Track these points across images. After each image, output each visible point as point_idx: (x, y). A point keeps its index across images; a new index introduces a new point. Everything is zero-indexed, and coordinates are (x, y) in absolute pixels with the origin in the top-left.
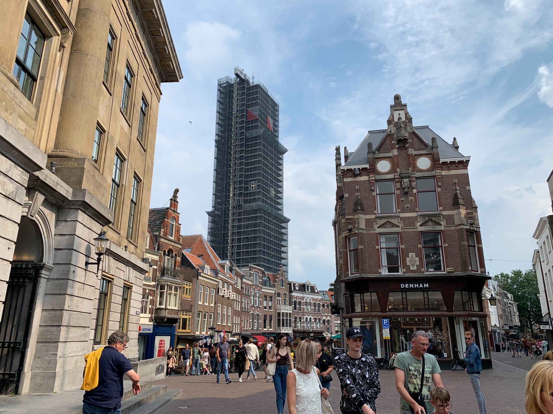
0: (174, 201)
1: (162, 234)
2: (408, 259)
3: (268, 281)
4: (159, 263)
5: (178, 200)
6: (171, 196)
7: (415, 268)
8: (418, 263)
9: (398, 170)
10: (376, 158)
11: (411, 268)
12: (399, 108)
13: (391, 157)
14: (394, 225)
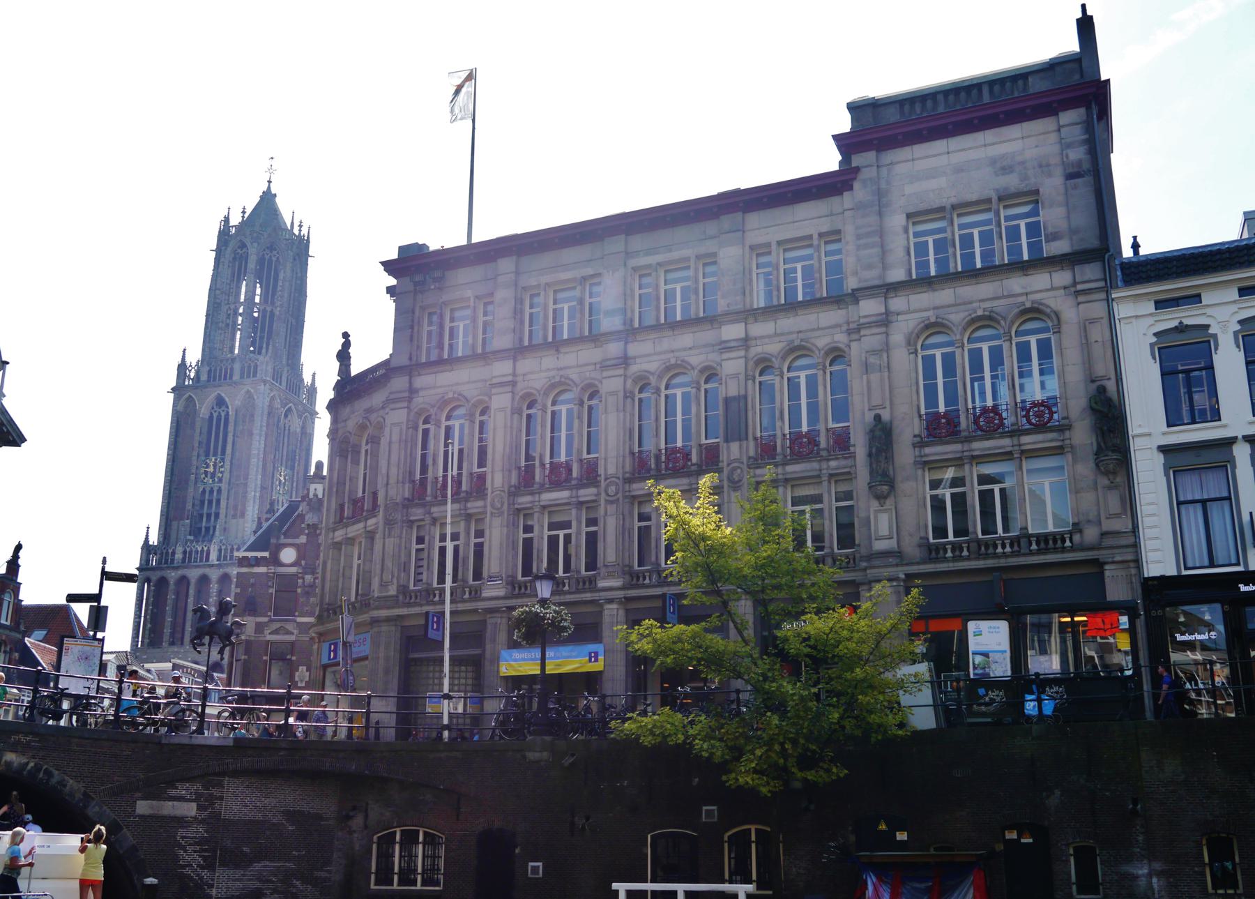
2: (297, 674)
5: (20, 562)
6: (9, 556)
7: (303, 685)
8: (307, 679)
9: (303, 562)
10: (280, 544)
11: (299, 685)
12: (317, 481)
13: (297, 544)
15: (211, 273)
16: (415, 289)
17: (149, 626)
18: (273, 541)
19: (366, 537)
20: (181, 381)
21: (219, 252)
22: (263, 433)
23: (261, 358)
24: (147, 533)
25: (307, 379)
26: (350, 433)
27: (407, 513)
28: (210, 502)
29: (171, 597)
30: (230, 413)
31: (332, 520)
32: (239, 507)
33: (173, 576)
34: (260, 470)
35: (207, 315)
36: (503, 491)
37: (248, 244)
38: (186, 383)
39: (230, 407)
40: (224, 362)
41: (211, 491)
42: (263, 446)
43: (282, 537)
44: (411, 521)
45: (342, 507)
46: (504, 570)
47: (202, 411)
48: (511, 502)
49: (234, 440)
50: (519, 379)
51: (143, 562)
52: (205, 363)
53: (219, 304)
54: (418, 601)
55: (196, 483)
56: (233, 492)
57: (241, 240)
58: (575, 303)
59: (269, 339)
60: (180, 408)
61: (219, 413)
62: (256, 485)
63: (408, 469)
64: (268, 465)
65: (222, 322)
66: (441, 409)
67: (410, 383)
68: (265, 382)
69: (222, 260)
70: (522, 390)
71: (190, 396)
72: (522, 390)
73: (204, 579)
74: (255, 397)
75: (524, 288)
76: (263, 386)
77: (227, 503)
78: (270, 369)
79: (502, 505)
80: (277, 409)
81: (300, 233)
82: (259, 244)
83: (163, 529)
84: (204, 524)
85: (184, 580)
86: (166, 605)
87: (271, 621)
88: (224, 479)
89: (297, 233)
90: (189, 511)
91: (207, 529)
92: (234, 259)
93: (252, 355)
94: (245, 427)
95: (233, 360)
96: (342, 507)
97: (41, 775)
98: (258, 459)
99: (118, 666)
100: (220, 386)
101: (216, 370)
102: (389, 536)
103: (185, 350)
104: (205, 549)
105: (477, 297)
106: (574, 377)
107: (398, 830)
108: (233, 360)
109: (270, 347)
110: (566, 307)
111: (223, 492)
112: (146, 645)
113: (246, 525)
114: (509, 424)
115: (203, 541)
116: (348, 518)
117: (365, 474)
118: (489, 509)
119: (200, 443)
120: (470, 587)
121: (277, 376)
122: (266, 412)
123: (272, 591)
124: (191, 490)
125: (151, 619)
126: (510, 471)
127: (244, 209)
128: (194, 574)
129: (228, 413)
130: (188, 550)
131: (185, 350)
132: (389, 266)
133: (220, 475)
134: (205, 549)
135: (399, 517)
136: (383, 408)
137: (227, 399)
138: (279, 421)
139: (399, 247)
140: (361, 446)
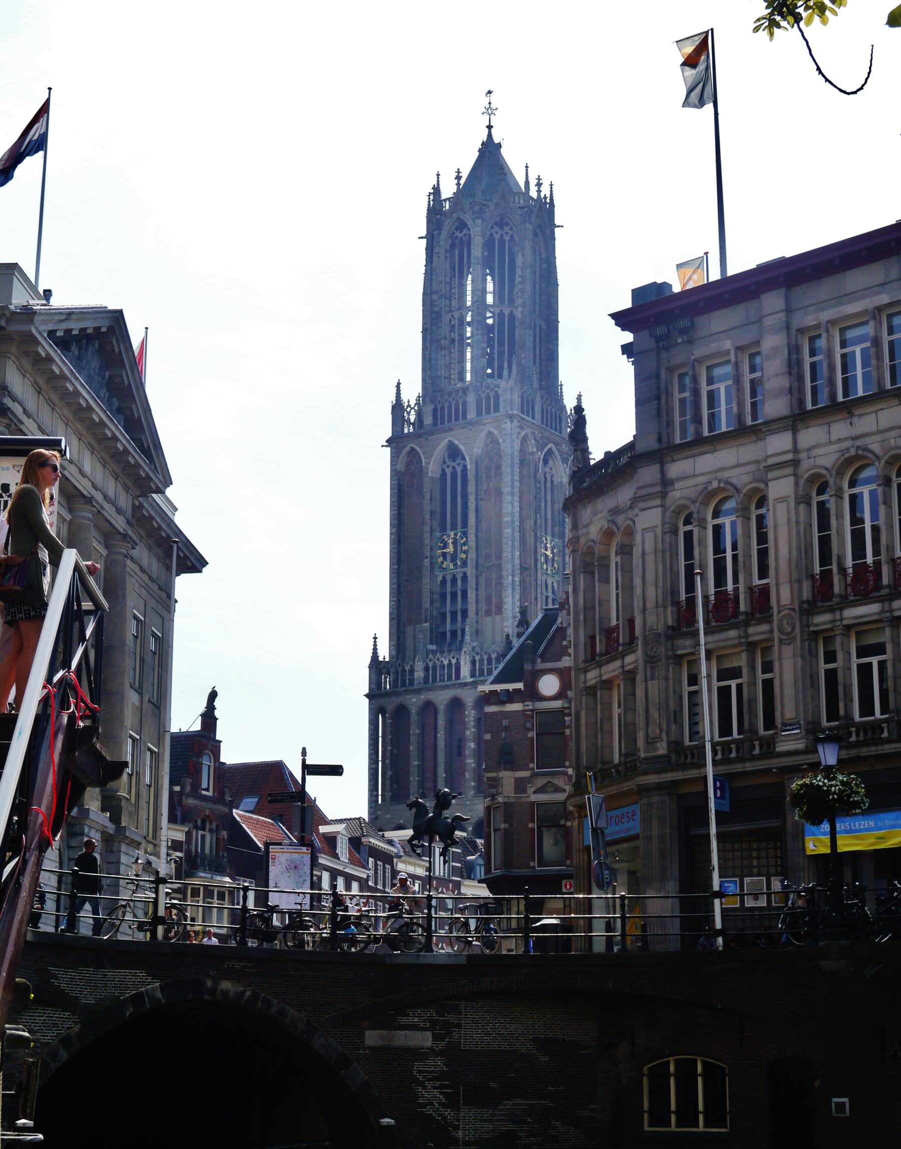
0: (209, 718)
1: (188, 789)
3: (480, 865)
4: (184, 847)
6: (202, 707)
13: (560, 669)
14: (558, 790)
15: (423, 270)
16: (658, 347)
17: (390, 773)
18: (528, 667)
19: (624, 679)
20: (399, 429)
21: (431, 238)
22: (516, 491)
23: (502, 383)
24: (375, 645)
25: (570, 403)
26: (593, 541)
27: (672, 645)
28: (454, 595)
29: (414, 731)
30: (469, 467)
31: (582, 657)
32: (494, 599)
33: (414, 702)
34: (517, 544)
35: (425, 331)
36: (794, 610)
37: (470, 223)
38: (406, 431)
39: (467, 458)
40: (454, 395)
41: (454, 580)
42: (518, 509)
43: (539, 660)
44: (678, 656)
45: (592, 638)
46: (802, 715)
47: (431, 468)
48: (805, 623)
49: (477, 506)
50: (803, 455)
51: (373, 686)
52: (428, 399)
53: (438, 313)
54: (696, 760)
55: (432, 570)
56: (482, 580)
57: (458, 218)
58: (868, 344)
59: (512, 352)
60: (400, 467)
61: (454, 468)
62: (513, 566)
63: (669, 588)
64: (528, 535)
65: (445, 338)
66: (705, 503)
67: (662, 472)
68: (511, 417)
69: (436, 250)
70: (808, 470)
71: (413, 449)
72: (808, 470)
73: (456, 704)
74: (501, 441)
75: (801, 331)
76: (509, 424)
77: (477, 595)
78: (517, 399)
79: (793, 628)
80: (533, 453)
81: (539, 195)
82: (483, 220)
83: (395, 638)
84: (448, 627)
85: (429, 708)
86: (408, 743)
87: (535, 775)
88: (469, 563)
89: (535, 197)
90: (427, 610)
91: (454, 633)
92: (453, 246)
93: (490, 381)
94: (491, 485)
95: (465, 390)
96: (592, 638)
97: (260, 1005)
98: (513, 529)
99: (349, 839)
100: (451, 430)
101: (442, 409)
102: (652, 679)
103: (399, 384)
104: (454, 661)
105: (739, 349)
106: (876, 447)
107: (671, 1059)
108: (465, 390)
109: (514, 366)
110: (858, 350)
111: (469, 579)
112: (388, 801)
113: (505, 624)
114: (794, 519)
115: (450, 651)
116: (601, 655)
117: (617, 594)
118: (776, 634)
119: (432, 513)
120: (761, 740)
121: (527, 406)
122: (517, 460)
123: (532, 734)
124: (426, 580)
125: (391, 763)
126: (800, 582)
127: (458, 172)
128: (441, 698)
129: (465, 467)
130: (431, 664)
131: (399, 384)
132: (621, 319)
133: (463, 556)
134: (454, 661)
135: (663, 653)
136: (631, 507)
137: (462, 448)
138: (536, 471)
139: (633, 291)
140: (609, 558)
